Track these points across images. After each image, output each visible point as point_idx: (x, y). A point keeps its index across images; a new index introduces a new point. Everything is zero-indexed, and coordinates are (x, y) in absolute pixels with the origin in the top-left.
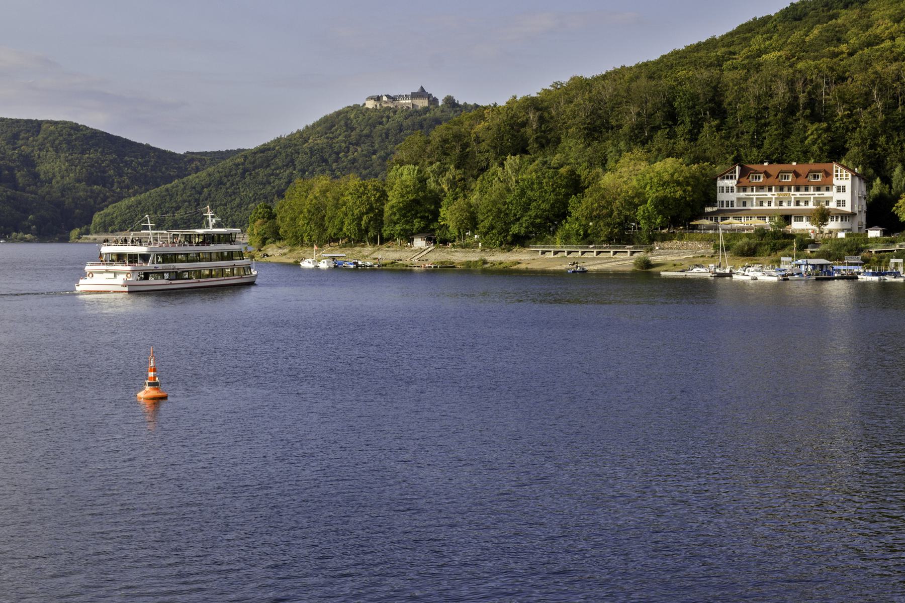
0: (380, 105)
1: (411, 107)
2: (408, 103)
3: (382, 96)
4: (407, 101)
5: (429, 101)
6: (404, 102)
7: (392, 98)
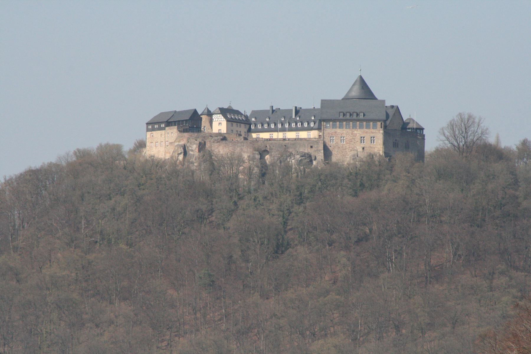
0: (202, 147)
1: (320, 156)
3: (210, 114)
4: (303, 135)
5: (387, 134)
6: (291, 135)
7: (247, 122)
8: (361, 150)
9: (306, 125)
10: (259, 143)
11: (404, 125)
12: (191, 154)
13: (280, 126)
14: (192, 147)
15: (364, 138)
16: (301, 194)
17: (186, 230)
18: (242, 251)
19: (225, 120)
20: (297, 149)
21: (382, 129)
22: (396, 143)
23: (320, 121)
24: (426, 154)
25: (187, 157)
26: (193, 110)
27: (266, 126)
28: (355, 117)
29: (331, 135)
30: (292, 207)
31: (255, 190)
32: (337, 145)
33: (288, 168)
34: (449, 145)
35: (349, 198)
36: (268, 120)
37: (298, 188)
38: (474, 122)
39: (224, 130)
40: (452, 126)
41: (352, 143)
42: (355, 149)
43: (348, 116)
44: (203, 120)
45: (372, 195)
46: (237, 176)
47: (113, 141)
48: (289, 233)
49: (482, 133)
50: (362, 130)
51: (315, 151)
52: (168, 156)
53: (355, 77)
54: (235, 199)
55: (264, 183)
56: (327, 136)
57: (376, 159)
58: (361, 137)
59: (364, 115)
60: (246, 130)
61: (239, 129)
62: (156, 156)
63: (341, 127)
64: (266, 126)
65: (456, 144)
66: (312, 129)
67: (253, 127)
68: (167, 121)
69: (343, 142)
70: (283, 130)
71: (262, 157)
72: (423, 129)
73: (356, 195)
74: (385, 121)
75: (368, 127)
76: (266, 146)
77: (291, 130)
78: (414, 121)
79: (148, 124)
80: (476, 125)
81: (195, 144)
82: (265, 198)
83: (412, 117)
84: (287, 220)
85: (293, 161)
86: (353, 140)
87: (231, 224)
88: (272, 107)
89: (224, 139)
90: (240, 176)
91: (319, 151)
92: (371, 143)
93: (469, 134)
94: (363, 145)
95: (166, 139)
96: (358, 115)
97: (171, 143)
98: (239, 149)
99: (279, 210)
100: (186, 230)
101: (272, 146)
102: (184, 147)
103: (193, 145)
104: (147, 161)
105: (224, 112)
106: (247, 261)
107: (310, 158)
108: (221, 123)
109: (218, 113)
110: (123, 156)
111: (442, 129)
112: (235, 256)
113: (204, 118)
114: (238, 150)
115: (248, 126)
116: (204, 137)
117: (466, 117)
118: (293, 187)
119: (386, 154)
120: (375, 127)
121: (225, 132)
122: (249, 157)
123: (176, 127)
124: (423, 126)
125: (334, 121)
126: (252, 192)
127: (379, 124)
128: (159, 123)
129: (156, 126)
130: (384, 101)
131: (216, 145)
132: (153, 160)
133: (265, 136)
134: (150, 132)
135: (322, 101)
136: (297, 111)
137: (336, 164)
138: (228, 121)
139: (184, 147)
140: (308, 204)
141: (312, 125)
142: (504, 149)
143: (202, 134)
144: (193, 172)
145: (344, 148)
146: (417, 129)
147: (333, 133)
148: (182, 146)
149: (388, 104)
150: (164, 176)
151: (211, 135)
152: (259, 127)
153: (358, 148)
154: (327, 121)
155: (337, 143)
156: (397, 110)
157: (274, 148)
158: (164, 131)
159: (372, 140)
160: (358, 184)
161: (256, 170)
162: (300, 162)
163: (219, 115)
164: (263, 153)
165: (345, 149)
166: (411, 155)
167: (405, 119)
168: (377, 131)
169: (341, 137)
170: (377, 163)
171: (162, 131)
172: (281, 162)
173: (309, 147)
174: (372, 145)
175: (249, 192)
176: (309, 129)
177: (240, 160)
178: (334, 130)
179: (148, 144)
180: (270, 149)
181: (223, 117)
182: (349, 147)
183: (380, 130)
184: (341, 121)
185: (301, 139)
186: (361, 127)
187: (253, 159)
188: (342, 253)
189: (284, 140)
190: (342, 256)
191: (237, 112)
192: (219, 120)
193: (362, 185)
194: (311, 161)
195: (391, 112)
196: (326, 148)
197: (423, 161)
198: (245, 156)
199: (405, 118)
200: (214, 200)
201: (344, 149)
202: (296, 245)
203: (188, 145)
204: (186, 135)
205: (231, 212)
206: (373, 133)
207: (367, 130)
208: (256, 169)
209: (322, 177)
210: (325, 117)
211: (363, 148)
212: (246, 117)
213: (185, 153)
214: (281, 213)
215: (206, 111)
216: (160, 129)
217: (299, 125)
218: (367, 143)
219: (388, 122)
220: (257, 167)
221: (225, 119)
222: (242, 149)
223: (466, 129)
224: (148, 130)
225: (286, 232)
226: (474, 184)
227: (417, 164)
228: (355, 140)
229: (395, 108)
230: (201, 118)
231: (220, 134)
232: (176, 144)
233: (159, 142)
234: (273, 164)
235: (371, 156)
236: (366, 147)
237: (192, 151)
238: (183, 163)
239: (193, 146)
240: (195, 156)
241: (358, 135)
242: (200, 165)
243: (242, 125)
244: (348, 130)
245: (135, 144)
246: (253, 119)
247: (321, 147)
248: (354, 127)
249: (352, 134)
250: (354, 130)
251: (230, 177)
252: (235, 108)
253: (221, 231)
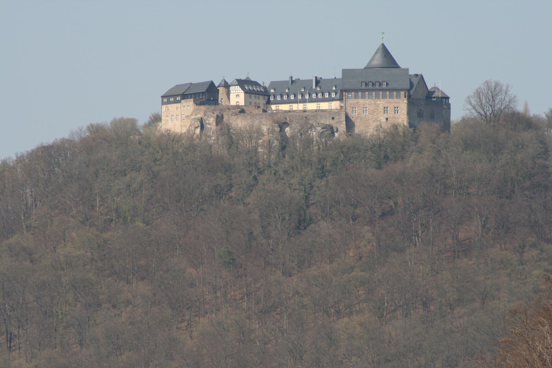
0: (219, 120)
1: (342, 127)
2: (332, 114)
3: (227, 86)
4: (324, 106)
5: (411, 103)
6: (311, 106)
7: (265, 93)
8: (384, 120)
9: (327, 95)
10: (279, 115)
11: (429, 95)
12: (209, 128)
13: (300, 97)
14: (209, 121)
15: (387, 108)
16: (323, 167)
17: (205, 207)
18: (263, 227)
19: (242, 91)
20: (318, 121)
21: (406, 98)
22: (420, 113)
23: (342, 91)
24: (452, 124)
25: (205, 131)
26: (210, 81)
27: (285, 97)
28: (377, 86)
29: (353, 105)
30: (314, 181)
31: (276, 164)
32: (359, 116)
33: (309, 141)
34: (476, 114)
35: (374, 171)
36: (287, 91)
37: (320, 161)
38: (501, 90)
39: (242, 103)
40: (478, 94)
41: (375, 113)
42: (379, 119)
43: (370, 86)
44: (220, 92)
45: (398, 167)
46: (256, 149)
47: (127, 115)
48: (311, 208)
49: (510, 101)
50: (385, 100)
51: (337, 122)
52: (184, 130)
53: (377, 46)
54: (255, 173)
55: (284, 157)
56: (349, 106)
57: (400, 129)
58: (385, 108)
59: (387, 84)
60: (265, 102)
61: (257, 101)
62: (172, 130)
63: (363, 97)
64: (285, 97)
65: (483, 112)
66: (334, 100)
67: (272, 99)
68: (182, 94)
69: (366, 113)
70: (303, 101)
71: (282, 130)
72: (448, 98)
73: (379, 167)
74: (409, 91)
75: (391, 97)
76: (286, 118)
77: (311, 101)
78: (439, 89)
79: (163, 97)
80: (503, 93)
81: (212, 117)
82: (286, 172)
83: (437, 86)
84: (309, 194)
85: (314, 134)
86: (376, 111)
87: (251, 199)
88: (292, 77)
89: (242, 111)
90: (260, 150)
91: (339, 122)
92: (395, 113)
93: (496, 102)
94: (386, 116)
95: (182, 113)
96: (380, 84)
97: (187, 117)
98: (257, 121)
99: (300, 184)
100: (205, 207)
101: (291, 118)
102: (201, 121)
103: (210, 118)
104: (162, 135)
105: (241, 83)
106: (269, 237)
107: (331, 130)
108: (239, 95)
109: (236, 84)
110: (138, 131)
111: (469, 97)
112: (255, 233)
113: (221, 90)
114: (257, 122)
115: (266, 98)
116: (222, 110)
117: (493, 84)
118: (315, 159)
119: (411, 125)
120: (398, 97)
121: (243, 104)
122: (268, 129)
123: (192, 100)
124: (449, 95)
125: (356, 91)
126: (272, 165)
127: (402, 93)
128: (175, 96)
129: (172, 99)
130: (407, 70)
131: (234, 117)
132: (169, 134)
133: (285, 107)
134: (166, 106)
135: (343, 70)
136: (318, 82)
137: (359, 135)
138: (246, 92)
139: (201, 121)
140: (330, 177)
141: (333, 95)
142: (533, 118)
143: (219, 107)
144: (210, 146)
145: (367, 119)
146: (442, 98)
147: (355, 103)
148: (199, 120)
149: (411, 72)
150: (180, 151)
151: (229, 108)
152: (279, 98)
153: (381, 119)
154: (348, 91)
155: (359, 114)
156: (421, 78)
158: (180, 104)
159: (396, 109)
160: (382, 156)
161: (276, 143)
162: (321, 134)
163: (237, 87)
164: (282, 125)
165: (368, 120)
166: (436, 125)
167: (429, 88)
168: (401, 101)
169: (364, 108)
170: (401, 133)
171: (177, 104)
172: (301, 135)
174: (396, 115)
175: (270, 166)
176: (331, 100)
177: (260, 133)
178: (355, 101)
179: (163, 118)
180: (290, 121)
181: (240, 89)
182: (372, 118)
183: (403, 100)
184: (363, 91)
185: (323, 111)
186: (384, 97)
187: (272, 131)
188: (367, 228)
189: (305, 111)
190: (366, 231)
191: (256, 84)
192: (237, 92)
193: (386, 157)
194: (333, 133)
195: (415, 81)
196: (348, 119)
197: (449, 132)
198: (265, 129)
199: (429, 88)
200: (233, 176)
201: (367, 120)
202: (319, 220)
203: (205, 118)
204: (203, 108)
205: (250, 188)
206: (396, 103)
207: (390, 100)
208: (275, 142)
209: (345, 150)
210: (347, 87)
211: (387, 119)
212: (265, 88)
213: (202, 127)
214: (303, 188)
215: (223, 83)
216: (176, 102)
217: (320, 96)
218: (390, 114)
219: (412, 92)
220: (277, 140)
221: (243, 91)
222: (261, 122)
223: (493, 97)
224: (163, 103)
225: (308, 207)
226: (502, 154)
227: (442, 135)
228: (378, 111)
229: (419, 77)
230: (218, 90)
231: (237, 106)
232: (193, 117)
233: (175, 115)
234: (293, 137)
235: (395, 127)
236: (390, 118)
237: (209, 124)
238: (200, 137)
239: (210, 119)
240: (212, 130)
241: (381, 105)
242: (218, 138)
243: (261, 97)
244: (371, 100)
245: (151, 118)
246: (272, 91)
247: (343, 118)
248: (377, 97)
249: (375, 104)
250: (376, 100)
251: (249, 151)
252: (253, 79)
253: (241, 207)
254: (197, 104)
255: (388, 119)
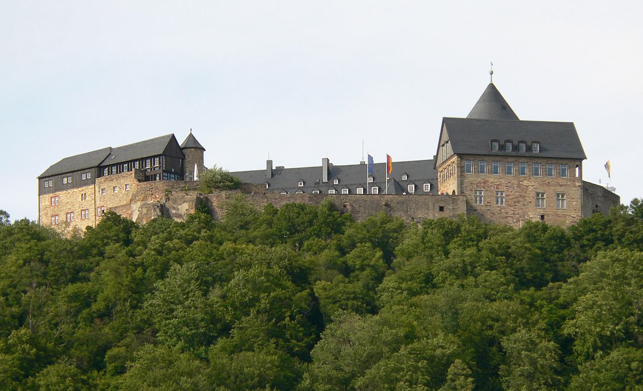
58: (538, 194)
86: (521, 199)
95: (98, 203)
134: (51, 195)
145: (504, 216)
147: (479, 182)
157: (362, 209)
171: (84, 188)
173: (438, 209)
178: (481, 178)
201: (503, 218)
203: (167, 205)
236: (548, 215)
239: (179, 207)
244: (510, 177)
249: (519, 186)
254: (139, 181)
255: (545, 217)
